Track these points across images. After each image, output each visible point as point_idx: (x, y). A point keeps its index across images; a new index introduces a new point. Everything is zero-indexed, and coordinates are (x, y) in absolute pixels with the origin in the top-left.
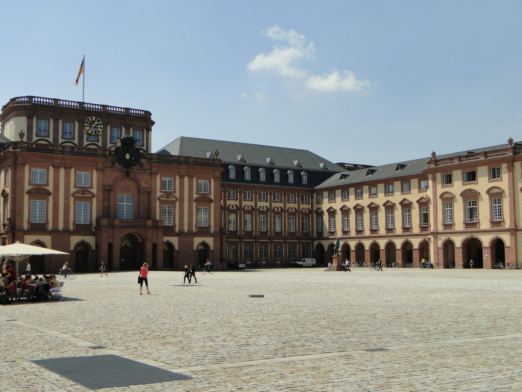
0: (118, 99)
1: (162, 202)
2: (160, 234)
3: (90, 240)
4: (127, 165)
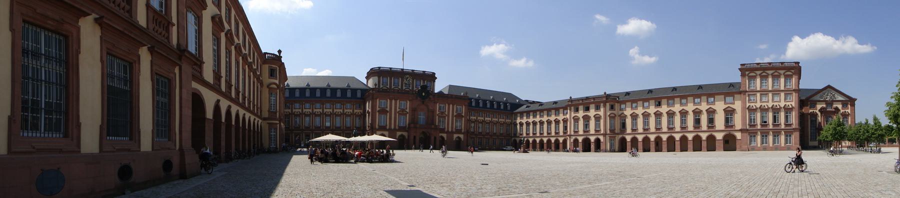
0: (419, 67)
3: (405, 134)
4: (423, 98)
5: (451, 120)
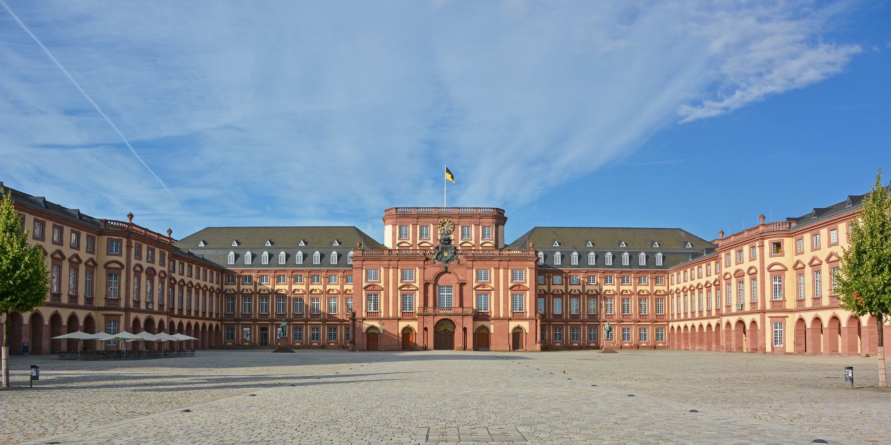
3: (414, 325)
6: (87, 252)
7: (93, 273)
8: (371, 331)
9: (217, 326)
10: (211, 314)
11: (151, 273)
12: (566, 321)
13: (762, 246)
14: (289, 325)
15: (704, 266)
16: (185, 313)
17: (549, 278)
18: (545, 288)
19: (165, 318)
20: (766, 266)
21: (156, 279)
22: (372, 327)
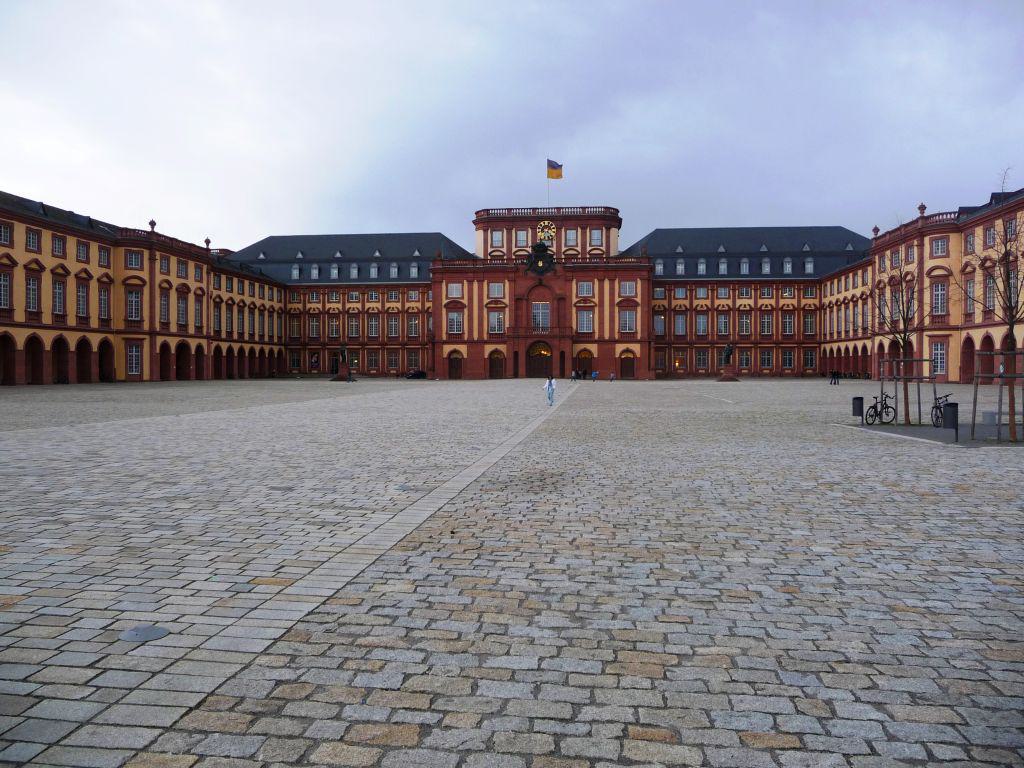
1: (579, 309)
2: (569, 342)
3: (502, 348)
5: (604, 311)
6: (100, 266)
7: (109, 291)
8: (455, 356)
9: (280, 352)
10: (271, 337)
11: (183, 291)
12: (691, 343)
13: (921, 246)
14: (286, 349)
15: (860, 272)
16: (235, 336)
17: (670, 290)
18: (665, 303)
19: (204, 342)
20: (926, 269)
21: (191, 298)
22: (455, 351)
